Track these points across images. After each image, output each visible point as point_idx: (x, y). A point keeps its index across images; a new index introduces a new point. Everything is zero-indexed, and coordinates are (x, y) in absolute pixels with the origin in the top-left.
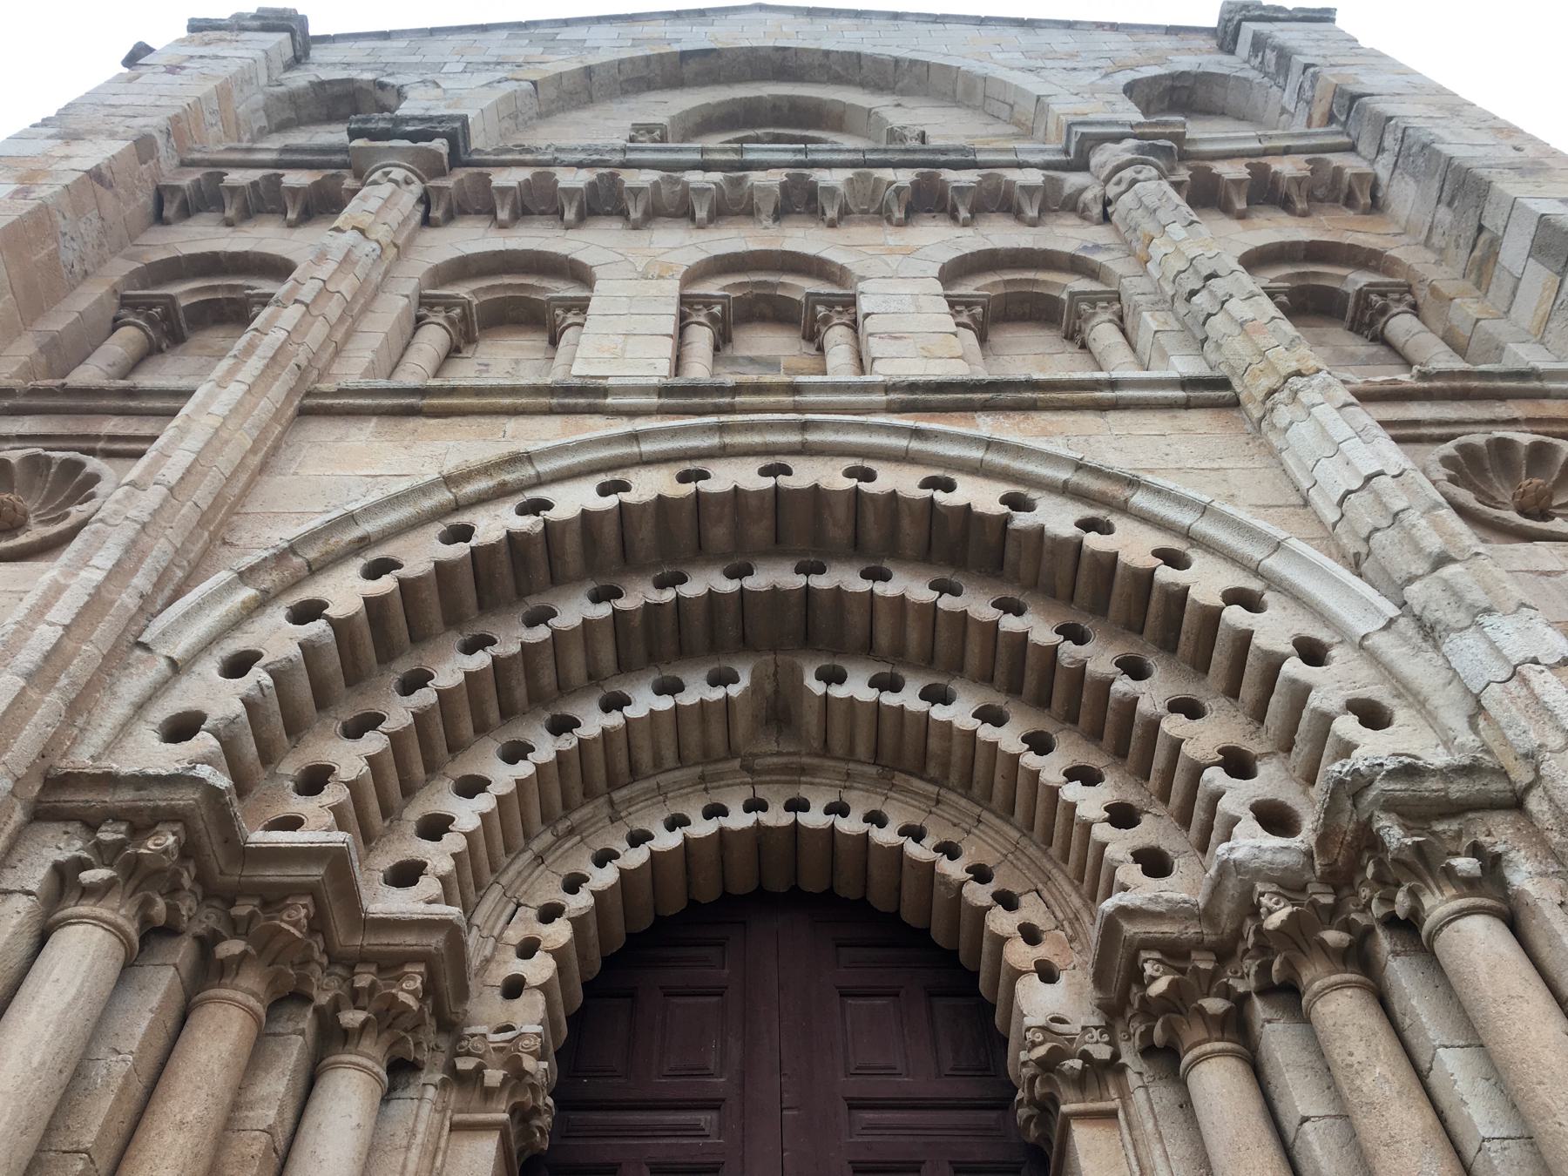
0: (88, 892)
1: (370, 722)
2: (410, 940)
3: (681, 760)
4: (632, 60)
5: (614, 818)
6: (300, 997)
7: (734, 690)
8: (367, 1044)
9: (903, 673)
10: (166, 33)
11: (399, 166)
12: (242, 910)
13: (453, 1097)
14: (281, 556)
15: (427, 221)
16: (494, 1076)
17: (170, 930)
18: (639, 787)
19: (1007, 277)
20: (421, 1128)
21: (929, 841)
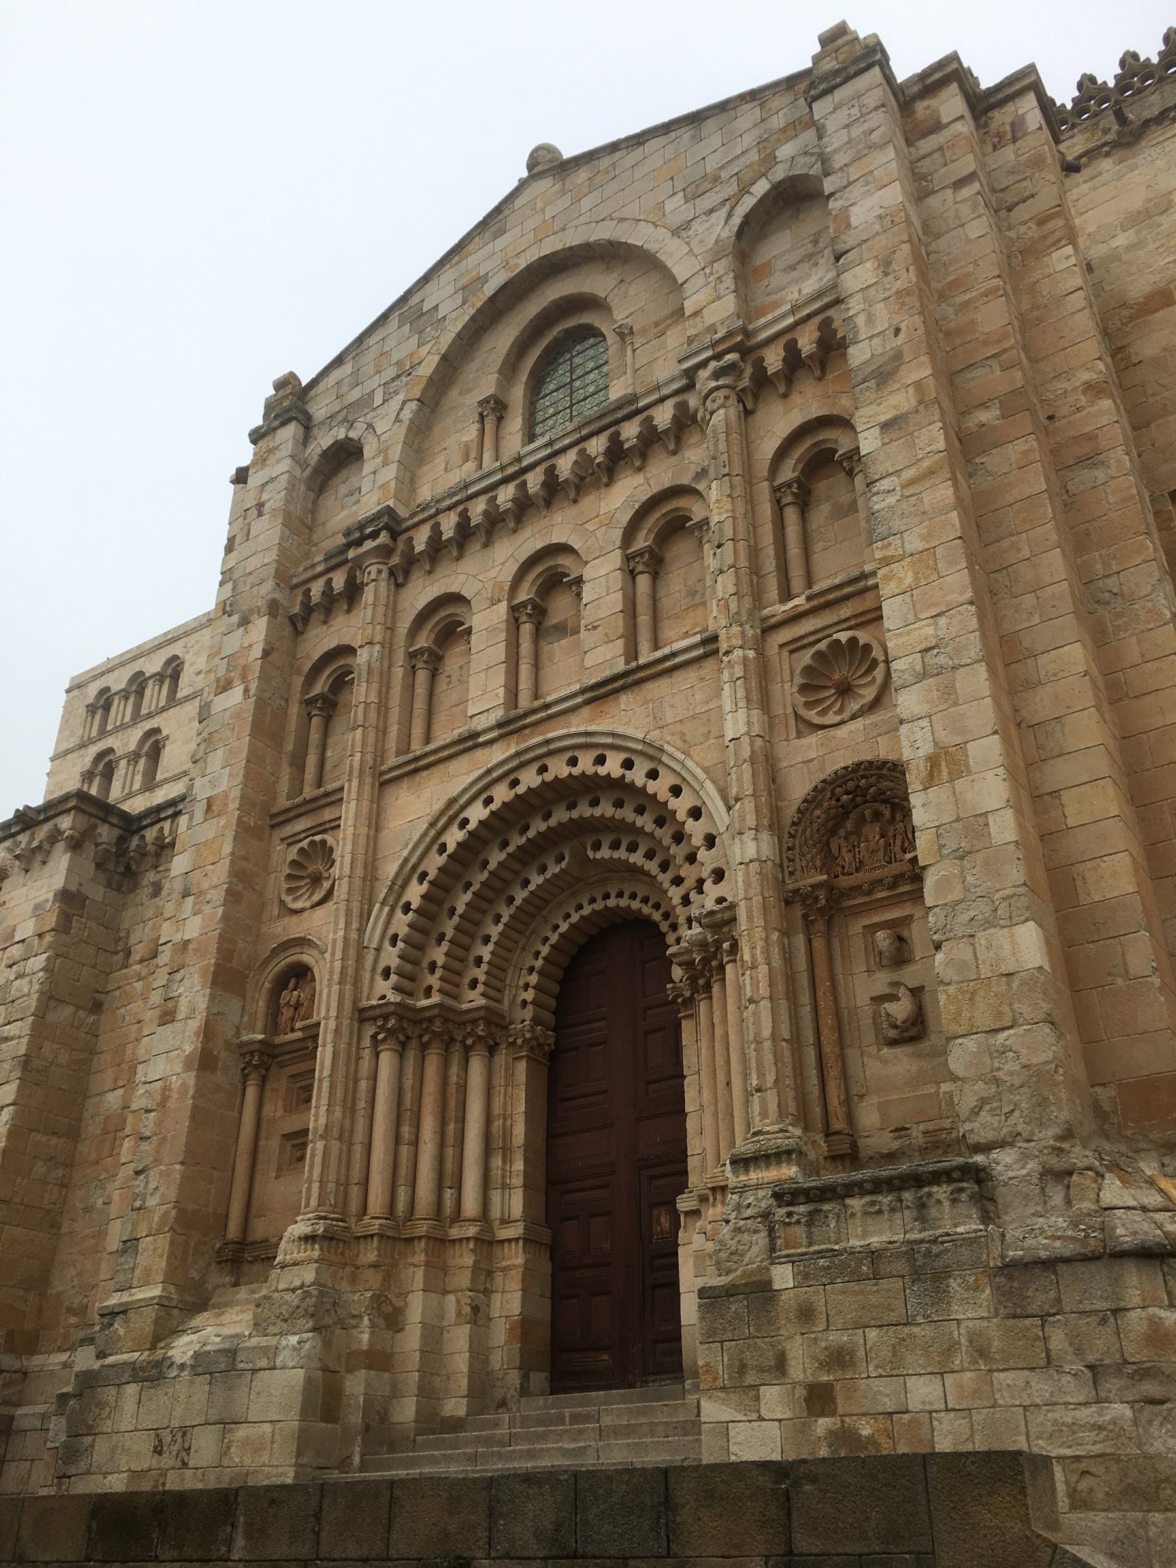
1: (442, 937)
2: (475, 1015)
6: (452, 1040)
7: (563, 865)
8: (477, 1047)
10: (245, 454)
12: (424, 1026)
14: (391, 888)
15: (398, 586)
16: (519, 1041)
17: (408, 1038)
19: (664, 511)
21: (650, 904)
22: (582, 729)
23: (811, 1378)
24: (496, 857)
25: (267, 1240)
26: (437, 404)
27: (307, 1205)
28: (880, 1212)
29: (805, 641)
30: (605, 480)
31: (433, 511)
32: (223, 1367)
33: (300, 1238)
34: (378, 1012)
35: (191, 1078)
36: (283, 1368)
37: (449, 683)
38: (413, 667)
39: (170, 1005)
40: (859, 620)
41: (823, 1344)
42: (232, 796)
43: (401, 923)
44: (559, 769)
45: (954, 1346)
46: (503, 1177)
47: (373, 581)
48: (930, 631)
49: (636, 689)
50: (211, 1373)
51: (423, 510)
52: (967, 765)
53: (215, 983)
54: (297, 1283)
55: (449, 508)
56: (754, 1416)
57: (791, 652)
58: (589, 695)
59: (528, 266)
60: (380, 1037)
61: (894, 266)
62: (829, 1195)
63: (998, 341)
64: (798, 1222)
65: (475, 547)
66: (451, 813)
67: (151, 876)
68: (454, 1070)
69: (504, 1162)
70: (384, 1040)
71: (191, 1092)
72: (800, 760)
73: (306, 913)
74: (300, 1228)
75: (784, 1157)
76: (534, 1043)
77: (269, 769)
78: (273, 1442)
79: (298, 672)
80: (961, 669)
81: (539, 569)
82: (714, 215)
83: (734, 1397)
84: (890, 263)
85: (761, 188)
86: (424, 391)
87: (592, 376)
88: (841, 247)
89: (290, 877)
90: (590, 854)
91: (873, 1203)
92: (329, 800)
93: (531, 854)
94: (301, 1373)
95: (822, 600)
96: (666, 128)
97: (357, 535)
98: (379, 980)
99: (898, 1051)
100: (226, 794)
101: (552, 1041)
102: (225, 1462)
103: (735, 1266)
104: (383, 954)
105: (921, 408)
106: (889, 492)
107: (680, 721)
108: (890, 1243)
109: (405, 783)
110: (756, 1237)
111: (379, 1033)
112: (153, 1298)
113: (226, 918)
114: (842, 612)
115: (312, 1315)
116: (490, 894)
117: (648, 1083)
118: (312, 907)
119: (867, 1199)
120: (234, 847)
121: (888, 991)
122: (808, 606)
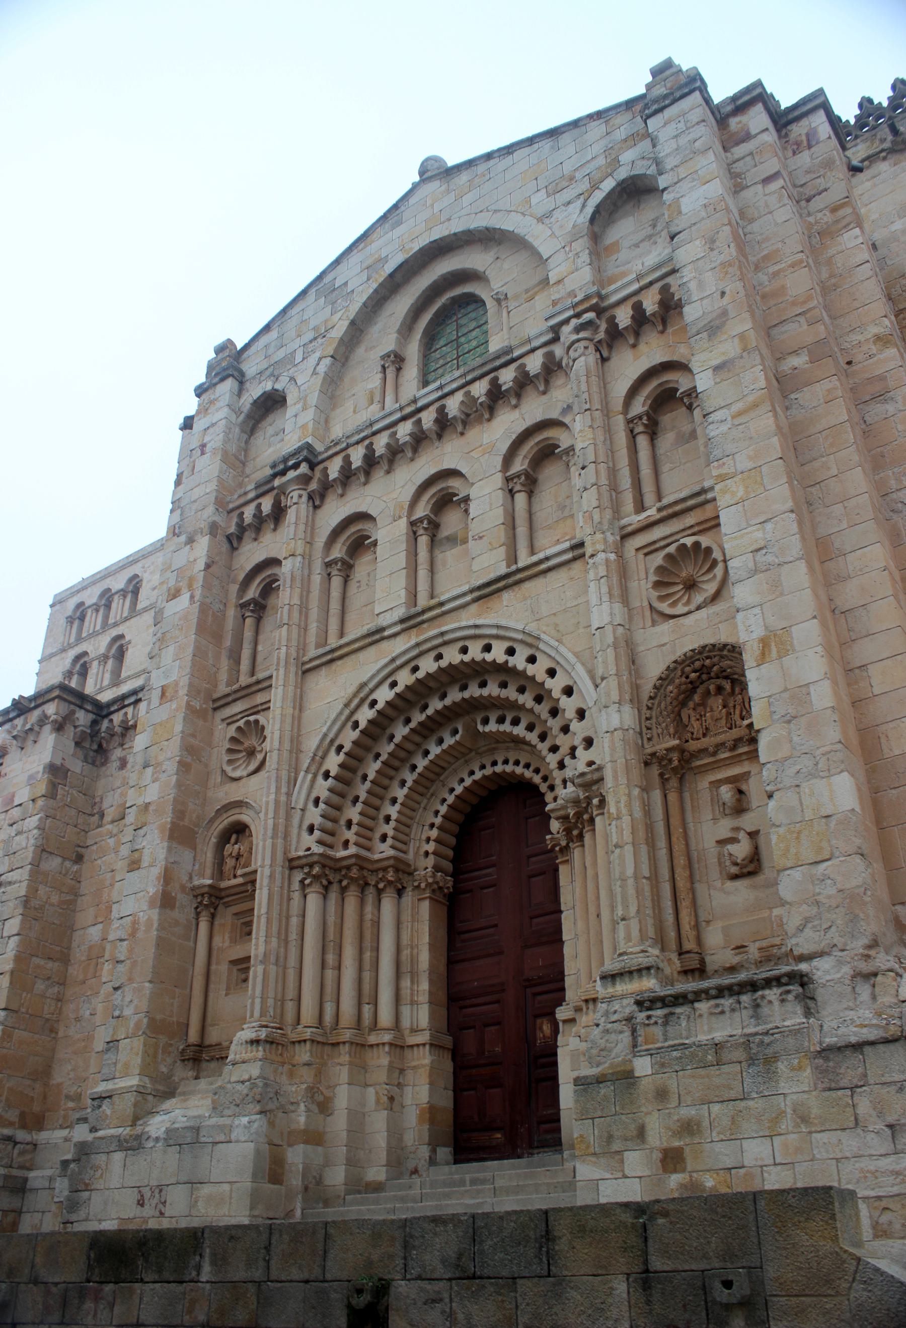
0: (309, 885)
2: (386, 863)
4: (369, 298)
5: (444, 786)
6: (367, 884)
7: (458, 737)
8: (388, 890)
9: (506, 713)
10: (191, 406)
11: (294, 490)
12: (343, 873)
13: (416, 892)
14: (313, 759)
15: (316, 507)
16: (423, 885)
17: (330, 883)
18: (447, 772)
21: (531, 769)
22: (471, 623)
23: (665, 1144)
24: (401, 731)
25: (220, 1044)
26: (347, 359)
27: (252, 1016)
28: (722, 1012)
29: (657, 545)
30: (487, 416)
31: (344, 445)
32: (189, 1140)
33: (246, 1042)
34: (304, 861)
35: (155, 914)
36: (237, 1141)
37: (359, 587)
38: (329, 574)
39: (136, 855)
40: (701, 527)
41: (676, 1118)
42: (181, 684)
43: (322, 788)
44: (452, 656)
45: (781, 1114)
46: (412, 994)
48: (759, 534)
49: (516, 588)
50: (180, 1145)
52: (792, 645)
53: (171, 838)
54: (246, 1077)
55: (358, 443)
56: (620, 1175)
57: (646, 554)
59: (421, 249)
60: (307, 882)
61: (717, 243)
62: (681, 1001)
63: (804, 303)
64: (656, 1023)
65: (378, 474)
66: (362, 695)
67: (118, 753)
68: (369, 909)
69: (412, 982)
70: (310, 885)
71: (155, 925)
72: (655, 644)
73: (244, 780)
74: (247, 1034)
75: (644, 972)
76: (435, 886)
77: (211, 662)
78: (231, 1198)
79: (234, 582)
80: (786, 566)
81: (433, 490)
82: (571, 206)
83: (602, 1160)
85: (608, 185)
86: (336, 350)
87: (474, 333)
88: (674, 229)
89: (230, 751)
90: (480, 728)
91: (717, 1006)
92: (260, 686)
93: (429, 729)
94: (252, 1145)
95: (670, 511)
96: (531, 141)
97: (281, 467)
98: (305, 834)
99: (739, 884)
100: (176, 683)
101: (450, 884)
102: (194, 1213)
103: (603, 1060)
104: (308, 814)
105: (745, 354)
106: (722, 421)
107: (554, 614)
108: (731, 1036)
109: (324, 671)
110: (621, 1036)
111: (305, 879)
112: (132, 1086)
113: (179, 785)
115: (259, 1102)
116: (396, 763)
117: (531, 918)
118: (249, 775)
119: (713, 1002)
120: (184, 726)
121: (729, 835)
122: (658, 516)
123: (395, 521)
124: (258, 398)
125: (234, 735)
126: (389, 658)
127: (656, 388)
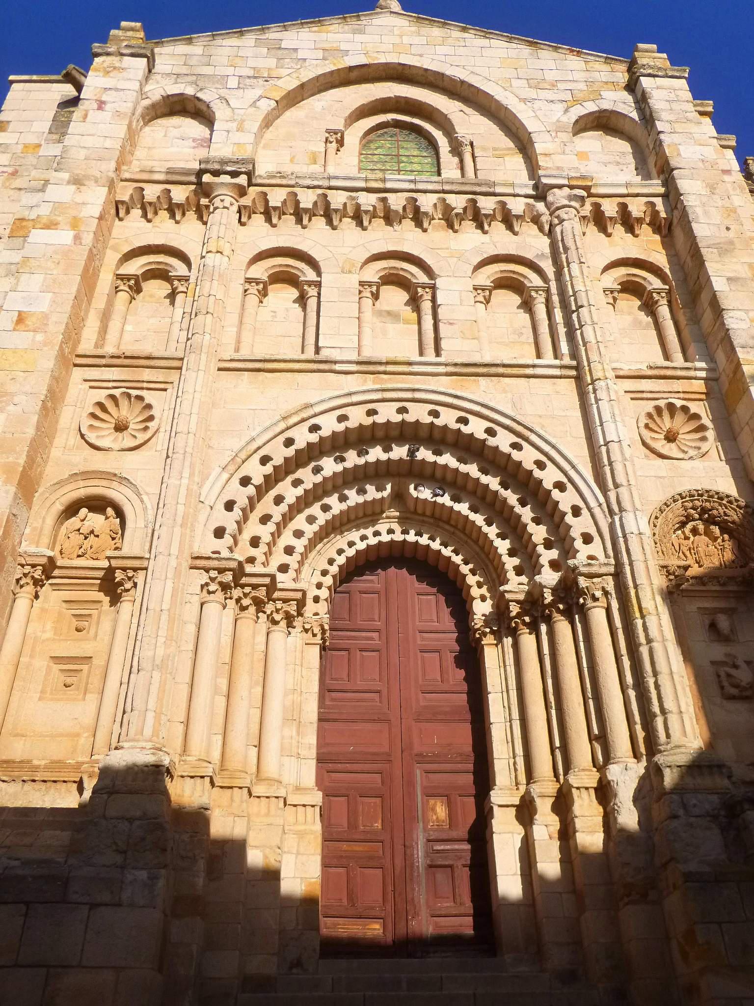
3: (365, 515)
4: (324, 75)
19: (503, 269)
20: (298, 645)
25: (29, 762)
29: (645, 395)
31: (292, 182)
34: (215, 564)
38: (246, 291)
42: (54, 318)
44: (419, 414)
47: (225, 208)
50: (27, 904)
51: (283, 177)
55: (308, 187)
57: (632, 399)
58: (450, 369)
59: (386, 64)
61: (717, 191)
66: (305, 415)
82: (552, 106)
84: (715, 188)
85: (591, 107)
86: (282, 98)
97: (217, 167)
100: (45, 316)
107: (540, 416)
114: (674, 386)
121: (724, 659)
123: (343, 272)
124: (172, 95)
125: (103, 401)
126: (346, 391)
127: (624, 276)
